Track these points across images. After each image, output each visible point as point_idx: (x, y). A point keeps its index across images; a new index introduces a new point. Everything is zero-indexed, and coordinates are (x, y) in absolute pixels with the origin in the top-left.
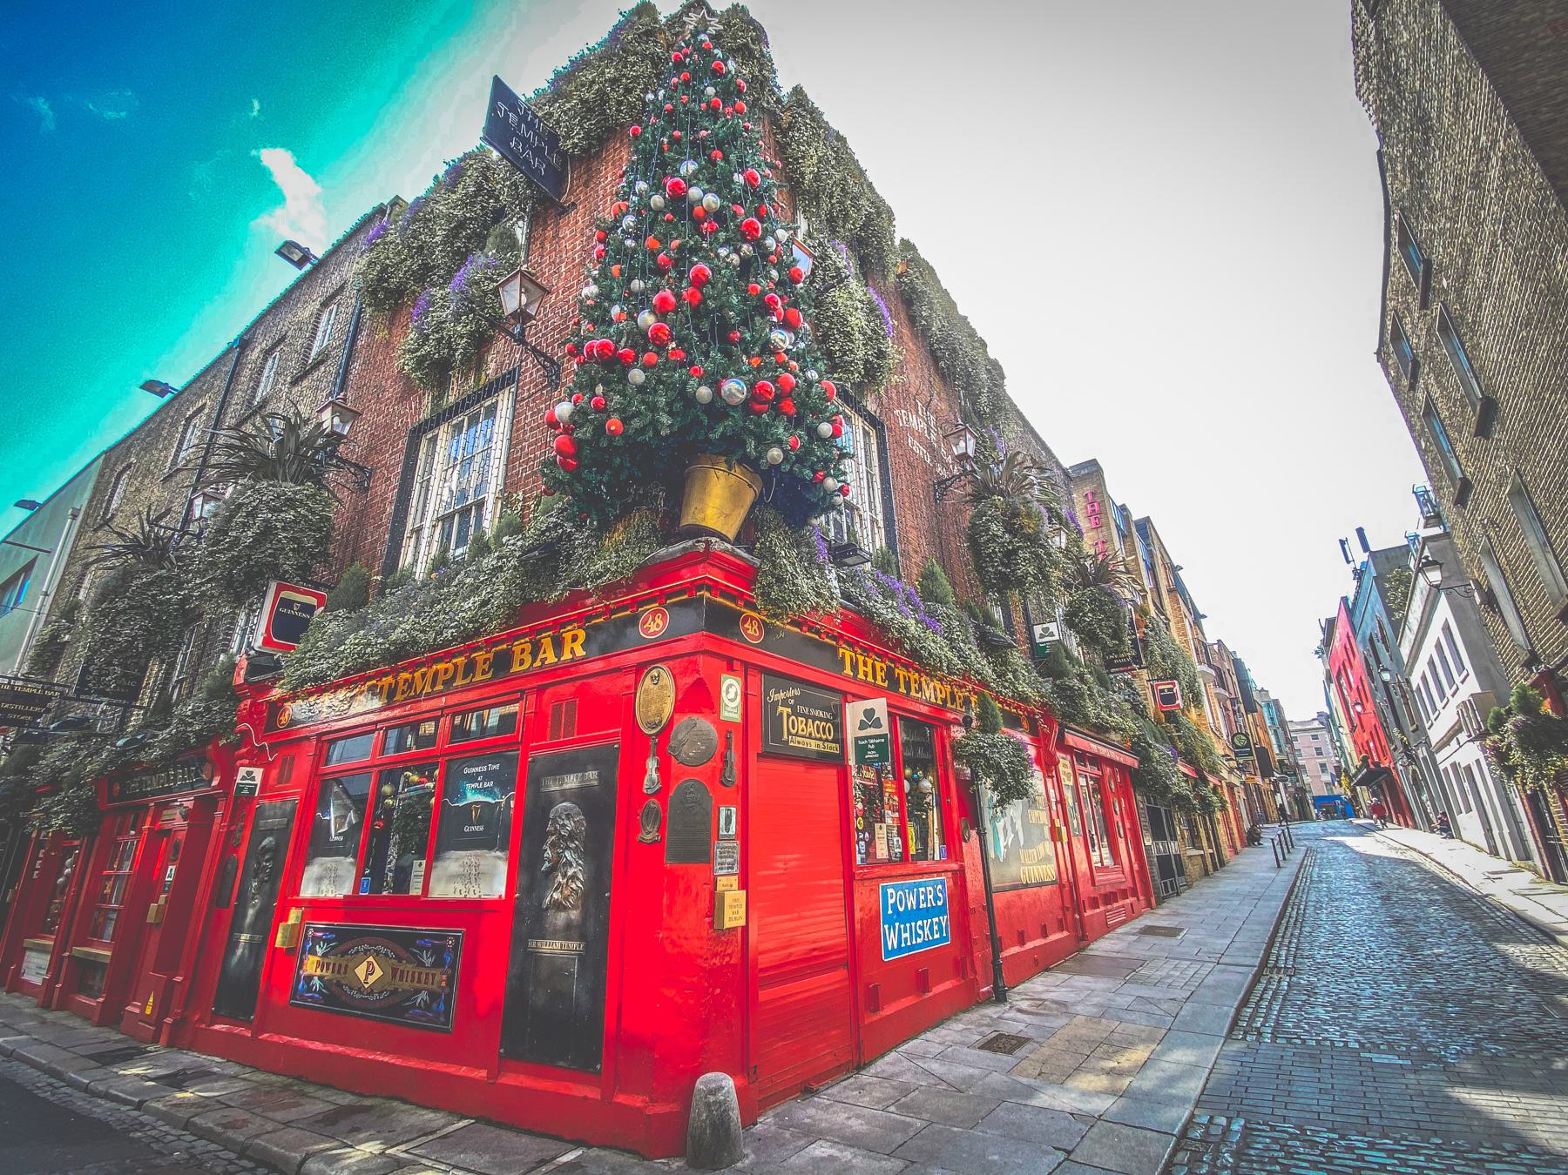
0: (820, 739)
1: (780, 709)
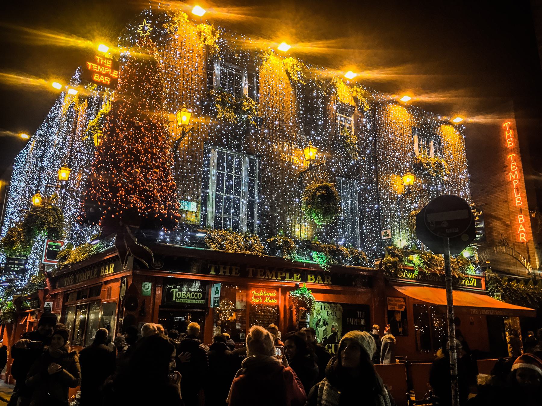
0: (194, 299)
1: (172, 290)
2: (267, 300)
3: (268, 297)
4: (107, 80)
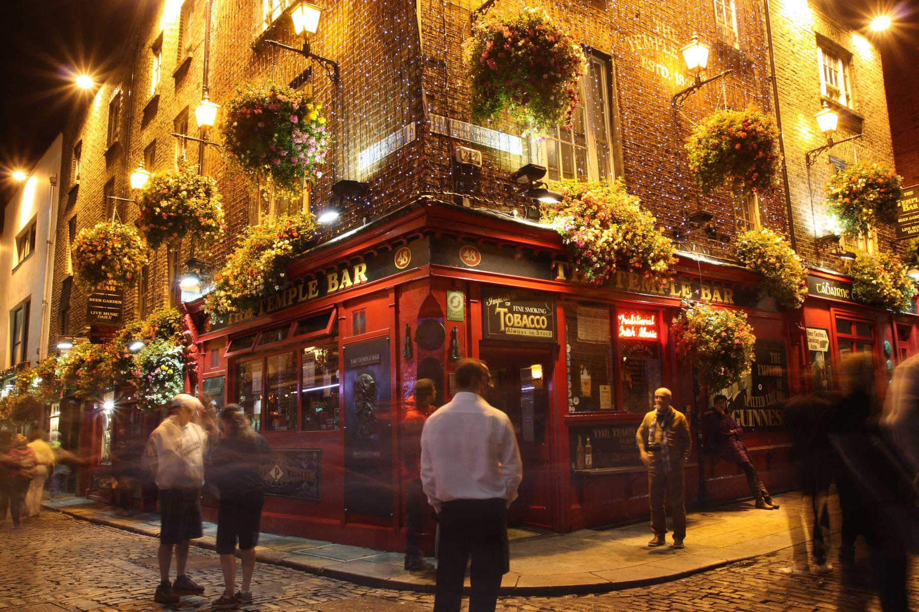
0: (535, 328)
1: (498, 309)
2: (644, 334)
3: (643, 326)
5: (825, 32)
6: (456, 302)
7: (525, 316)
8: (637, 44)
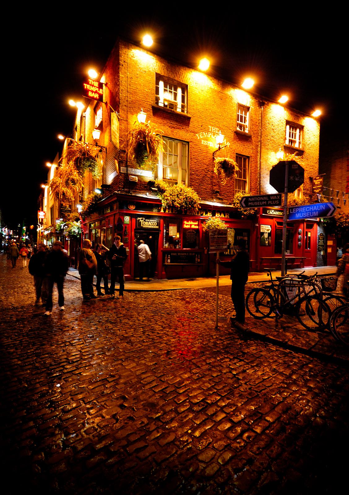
1: (140, 221)
2: (193, 227)
4: (96, 96)
5: (291, 119)
6: (127, 219)
7: (149, 222)
8: (199, 136)
